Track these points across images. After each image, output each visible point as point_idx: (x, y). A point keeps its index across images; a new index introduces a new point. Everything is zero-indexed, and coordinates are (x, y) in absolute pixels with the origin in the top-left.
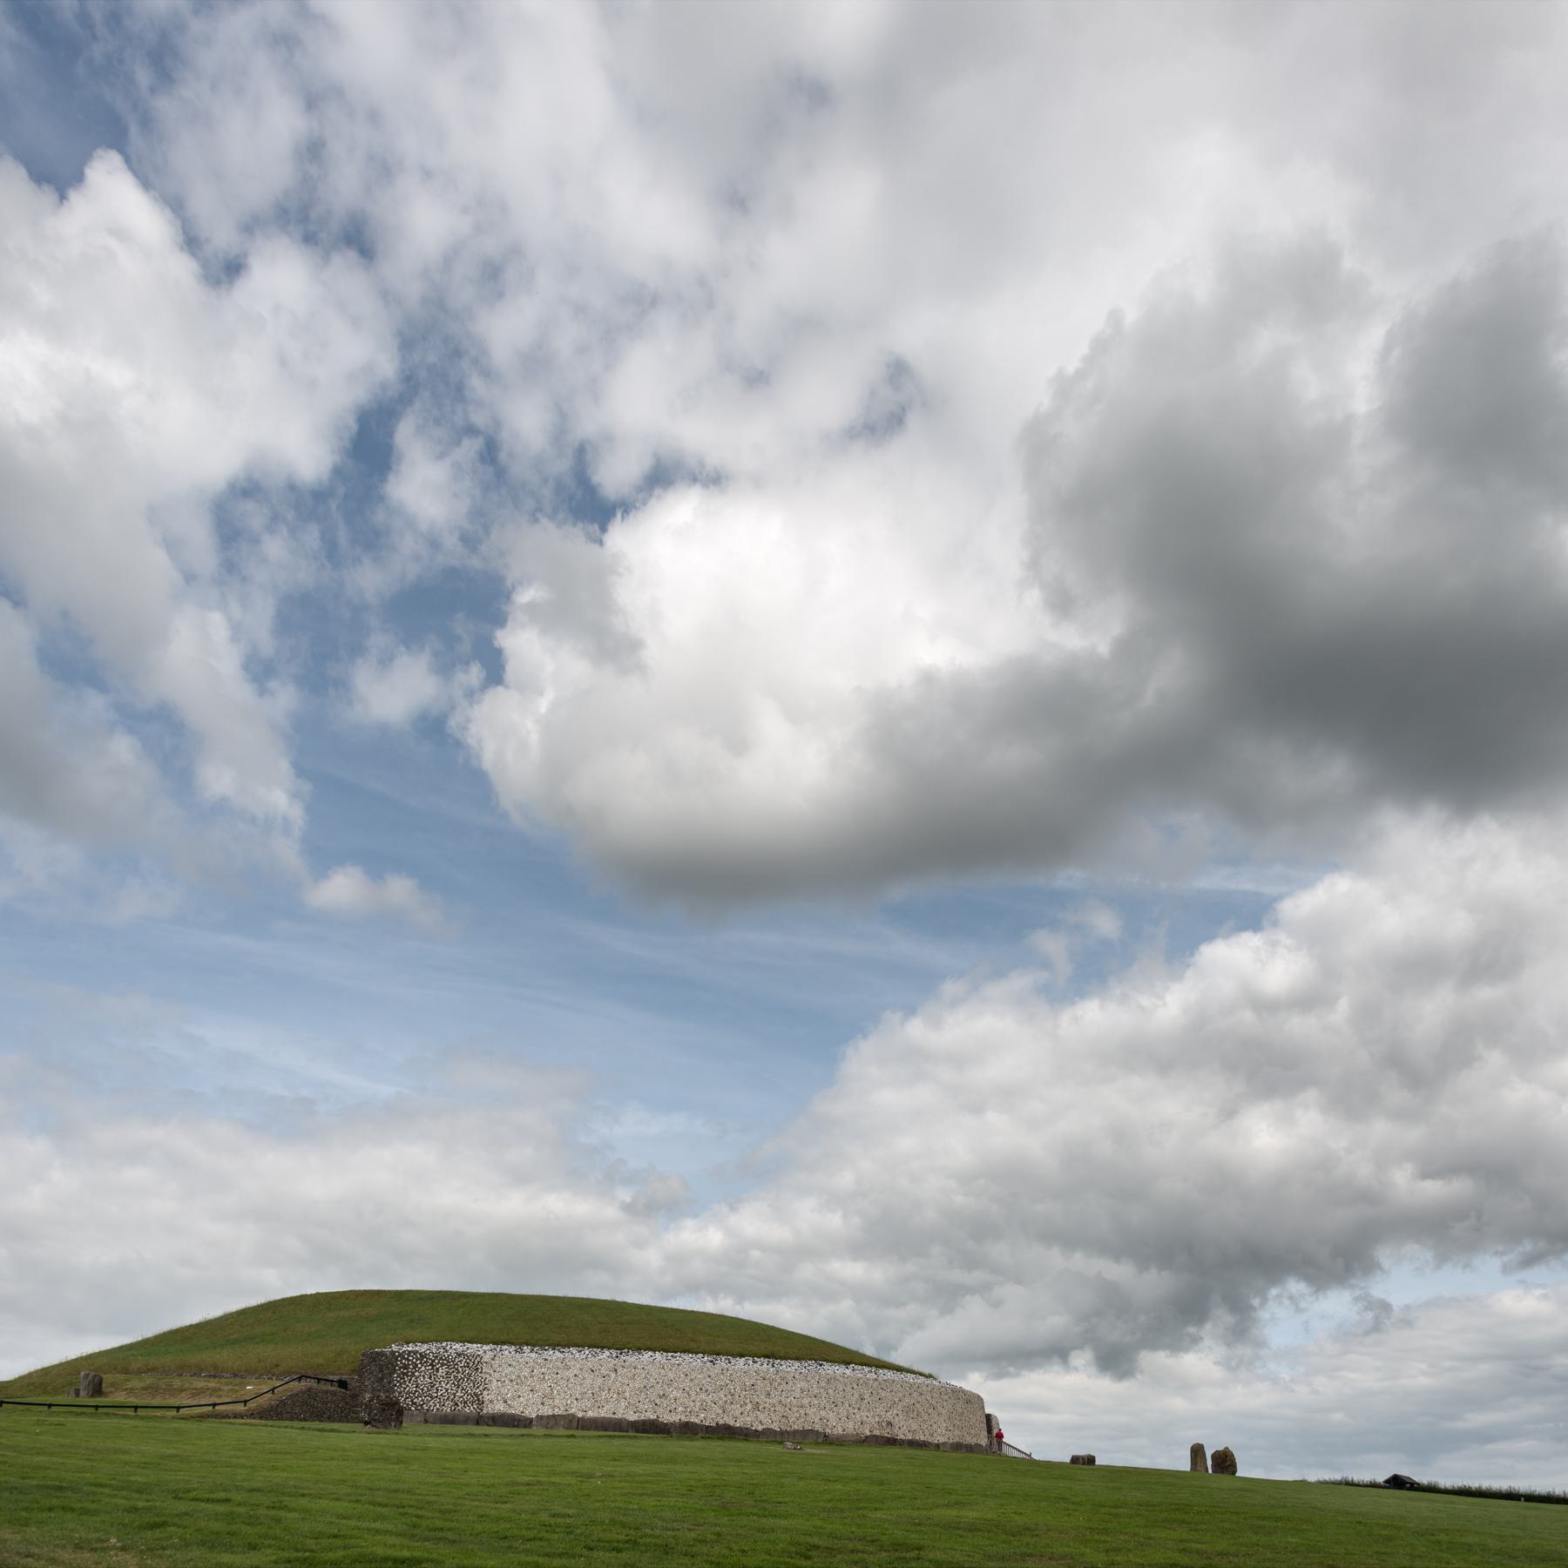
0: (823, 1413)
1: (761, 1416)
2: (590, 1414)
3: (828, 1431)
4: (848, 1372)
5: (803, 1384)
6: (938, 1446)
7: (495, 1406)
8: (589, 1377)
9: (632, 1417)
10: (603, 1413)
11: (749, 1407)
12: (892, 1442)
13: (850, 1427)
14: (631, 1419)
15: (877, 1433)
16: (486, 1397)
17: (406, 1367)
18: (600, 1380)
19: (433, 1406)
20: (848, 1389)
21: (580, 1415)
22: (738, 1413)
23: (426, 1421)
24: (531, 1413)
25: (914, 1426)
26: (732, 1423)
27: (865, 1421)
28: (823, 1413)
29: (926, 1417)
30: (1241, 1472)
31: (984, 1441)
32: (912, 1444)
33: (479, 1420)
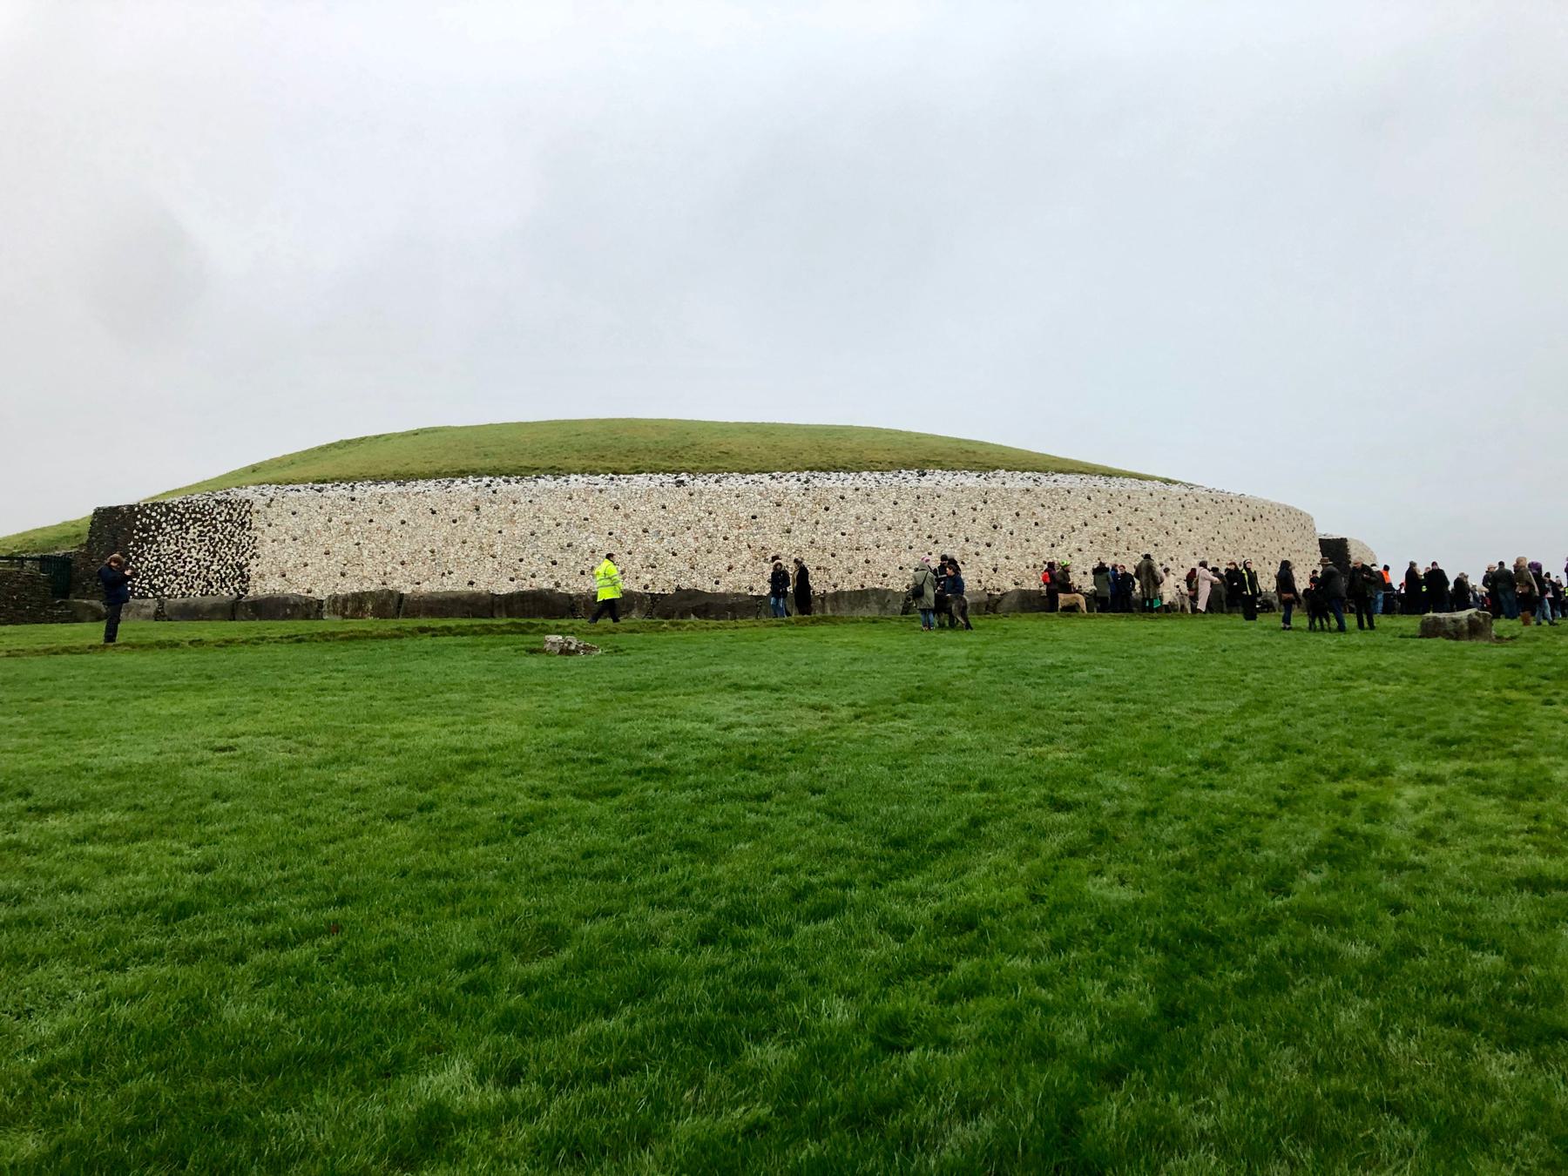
2: (426, 588)
5: (860, 509)
7: (265, 585)
8: (428, 522)
9: (505, 588)
10: (455, 584)
14: (504, 591)
16: (254, 568)
17: (146, 529)
18: (446, 529)
19: (175, 591)
20: (965, 513)
21: (407, 590)
22: (723, 569)
23: (159, 616)
24: (321, 592)
26: (708, 587)
33: (233, 610)
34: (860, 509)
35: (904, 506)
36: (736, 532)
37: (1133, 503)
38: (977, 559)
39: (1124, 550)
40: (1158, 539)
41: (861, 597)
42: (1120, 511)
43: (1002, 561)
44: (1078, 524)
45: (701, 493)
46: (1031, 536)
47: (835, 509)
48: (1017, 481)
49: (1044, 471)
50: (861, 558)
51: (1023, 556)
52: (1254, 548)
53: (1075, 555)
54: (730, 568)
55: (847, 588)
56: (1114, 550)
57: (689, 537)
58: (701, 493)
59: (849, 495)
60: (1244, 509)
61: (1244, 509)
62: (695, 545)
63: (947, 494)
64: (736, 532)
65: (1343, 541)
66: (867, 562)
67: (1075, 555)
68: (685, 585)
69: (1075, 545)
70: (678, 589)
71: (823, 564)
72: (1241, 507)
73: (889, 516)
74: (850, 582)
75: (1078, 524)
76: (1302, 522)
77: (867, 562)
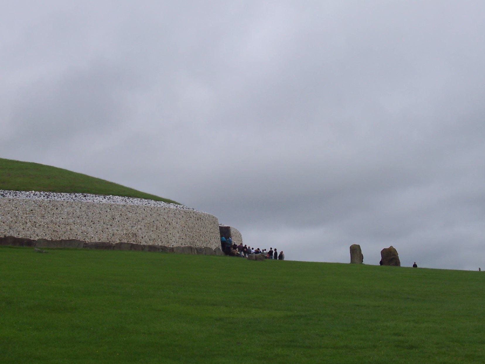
0: (84, 228)
1: (38, 231)
3: (87, 240)
4: (104, 201)
6: (172, 250)
11: (29, 224)
12: (134, 247)
13: (104, 238)
15: (125, 241)
25: (154, 236)
26: (16, 236)
27: (116, 234)
28: (84, 228)
29: (163, 230)
30: (402, 265)
31: (215, 243)
32: (152, 248)
34: (71, 210)
35: (83, 209)
36: (25, 215)
37: (159, 212)
38: (107, 230)
39: (155, 230)
40: (166, 226)
41: (70, 242)
42: (154, 215)
43: (116, 231)
44: (140, 219)
45: (13, 200)
46: (125, 222)
47: (60, 209)
48: (118, 200)
49: (129, 196)
50: (68, 228)
51: (122, 230)
52: (198, 231)
53: (139, 230)
54: (23, 229)
55: (63, 238)
56: (152, 229)
57: (9, 216)
58: (13, 200)
59: (65, 204)
60: (195, 216)
61: (195, 216)
62: (11, 220)
63: (98, 206)
64: (25, 215)
65: (229, 227)
66: (71, 229)
67: (139, 230)
68: (8, 235)
69: (139, 227)
70: (5, 236)
71: (56, 229)
72: (194, 215)
73: (79, 214)
74: (65, 236)
75: (140, 219)
76: (214, 221)
77: (71, 229)
